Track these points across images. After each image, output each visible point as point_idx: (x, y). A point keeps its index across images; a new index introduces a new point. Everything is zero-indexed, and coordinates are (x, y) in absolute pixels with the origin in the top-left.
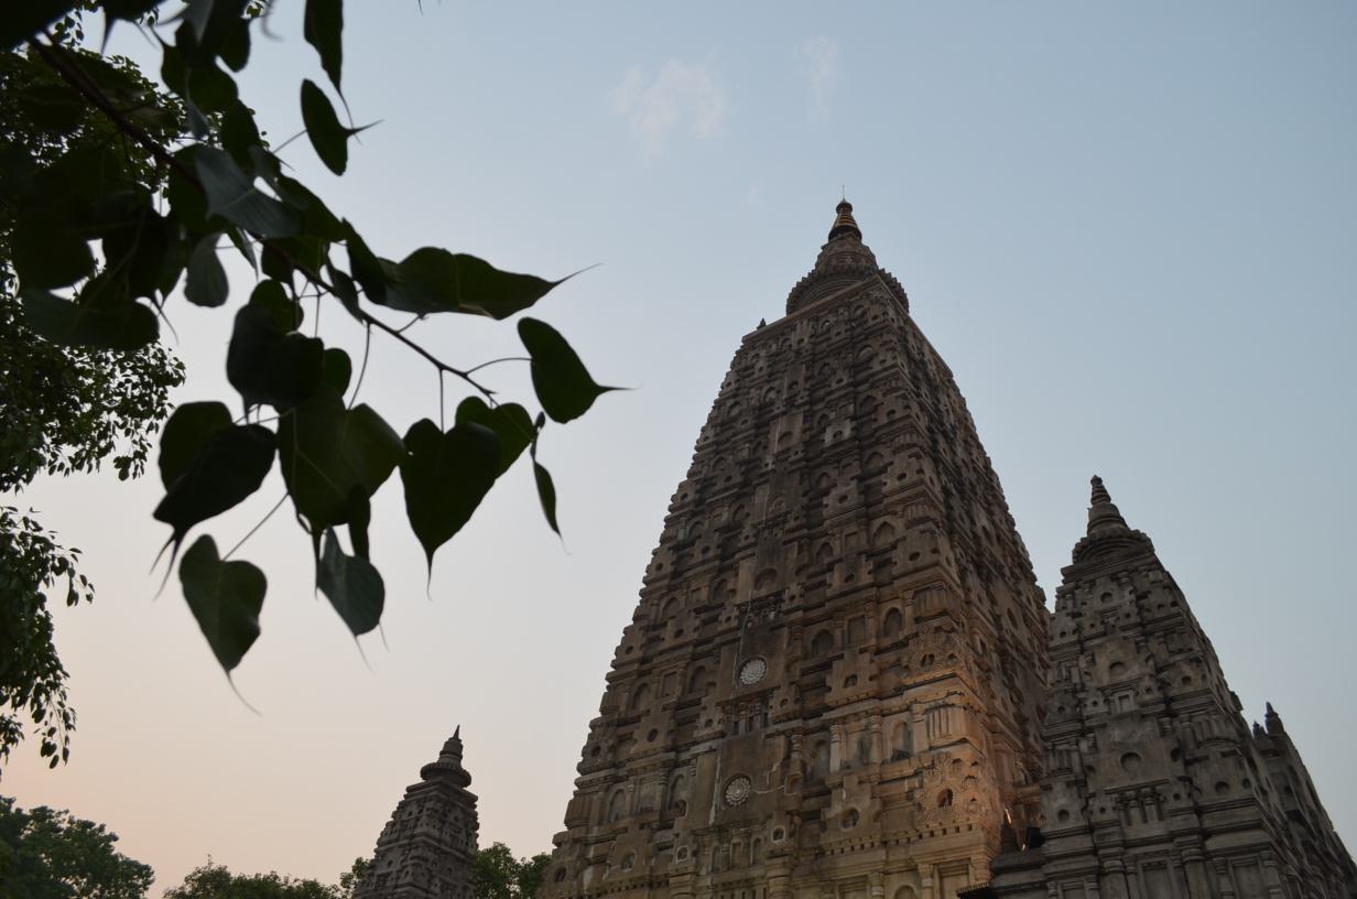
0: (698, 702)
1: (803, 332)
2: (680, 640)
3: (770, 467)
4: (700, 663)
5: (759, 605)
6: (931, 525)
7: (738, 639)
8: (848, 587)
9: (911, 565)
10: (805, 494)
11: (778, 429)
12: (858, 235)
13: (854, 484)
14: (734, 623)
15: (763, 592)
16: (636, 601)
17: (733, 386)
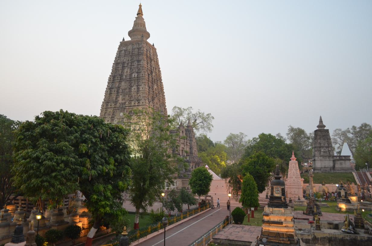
0: (114, 117)
1: (130, 47)
2: (111, 107)
3: (124, 78)
4: (114, 111)
5: (123, 104)
6: (146, 98)
7: (119, 109)
8: (134, 105)
9: (142, 104)
10: (129, 86)
11: (125, 70)
12: (142, 15)
13: (136, 87)
14: (119, 106)
15: (123, 102)
16: (104, 97)
17: (118, 55)
